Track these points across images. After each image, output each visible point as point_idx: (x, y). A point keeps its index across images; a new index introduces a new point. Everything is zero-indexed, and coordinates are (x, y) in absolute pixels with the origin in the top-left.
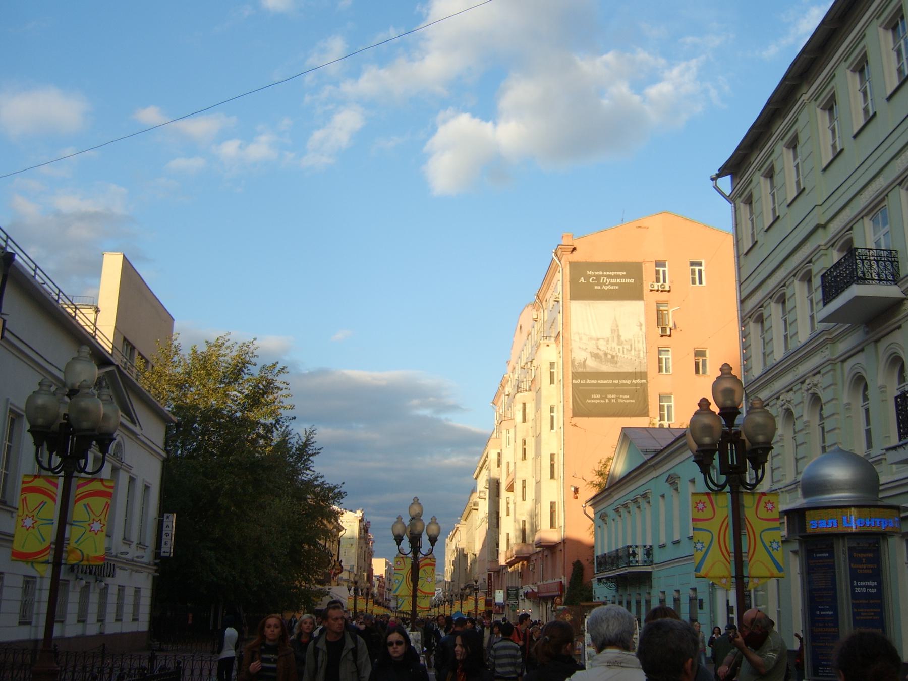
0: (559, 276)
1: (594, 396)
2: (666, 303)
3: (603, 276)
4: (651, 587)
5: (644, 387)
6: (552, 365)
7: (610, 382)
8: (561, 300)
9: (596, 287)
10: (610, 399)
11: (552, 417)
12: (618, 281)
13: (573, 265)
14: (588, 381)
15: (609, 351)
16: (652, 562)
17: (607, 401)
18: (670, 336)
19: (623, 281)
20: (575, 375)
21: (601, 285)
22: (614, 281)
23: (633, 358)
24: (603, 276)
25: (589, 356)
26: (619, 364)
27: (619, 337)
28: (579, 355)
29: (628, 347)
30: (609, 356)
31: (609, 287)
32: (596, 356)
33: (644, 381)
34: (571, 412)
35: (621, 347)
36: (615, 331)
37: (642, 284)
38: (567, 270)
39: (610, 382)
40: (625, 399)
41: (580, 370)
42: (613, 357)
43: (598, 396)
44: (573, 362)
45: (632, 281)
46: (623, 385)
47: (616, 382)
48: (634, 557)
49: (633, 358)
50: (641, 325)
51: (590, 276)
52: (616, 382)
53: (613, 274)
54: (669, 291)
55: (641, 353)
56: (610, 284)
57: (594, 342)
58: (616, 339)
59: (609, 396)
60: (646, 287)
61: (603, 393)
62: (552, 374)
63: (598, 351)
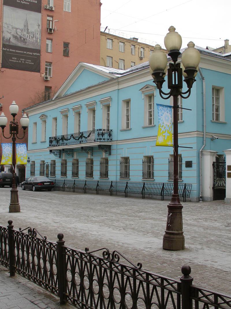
4: (110, 154)
5: (39, 57)
7: (22, 52)
10: (21, 61)
14: (11, 50)
15: (22, 36)
16: (111, 140)
20: (4, 46)
23: (34, 42)
25: (12, 37)
26: (27, 44)
27: (28, 30)
28: (7, 36)
29: (32, 36)
30: (22, 39)
32: (15, 37)
33: (39, 54)
36: (26, 26)
39: (22, 52)
40: (29, 62)
41: (7, 43)
42: (24, 39)
43: (16, 59)
44: (3, 38)
45: (36, 2)
47: (25, 52)
48: (103, 136)
49: (34, 42)
52: (25, 52)
55: (38, 40)
58: (26, 30)
59: (22, 60)
61: (19, 57)
63: (17, 35)
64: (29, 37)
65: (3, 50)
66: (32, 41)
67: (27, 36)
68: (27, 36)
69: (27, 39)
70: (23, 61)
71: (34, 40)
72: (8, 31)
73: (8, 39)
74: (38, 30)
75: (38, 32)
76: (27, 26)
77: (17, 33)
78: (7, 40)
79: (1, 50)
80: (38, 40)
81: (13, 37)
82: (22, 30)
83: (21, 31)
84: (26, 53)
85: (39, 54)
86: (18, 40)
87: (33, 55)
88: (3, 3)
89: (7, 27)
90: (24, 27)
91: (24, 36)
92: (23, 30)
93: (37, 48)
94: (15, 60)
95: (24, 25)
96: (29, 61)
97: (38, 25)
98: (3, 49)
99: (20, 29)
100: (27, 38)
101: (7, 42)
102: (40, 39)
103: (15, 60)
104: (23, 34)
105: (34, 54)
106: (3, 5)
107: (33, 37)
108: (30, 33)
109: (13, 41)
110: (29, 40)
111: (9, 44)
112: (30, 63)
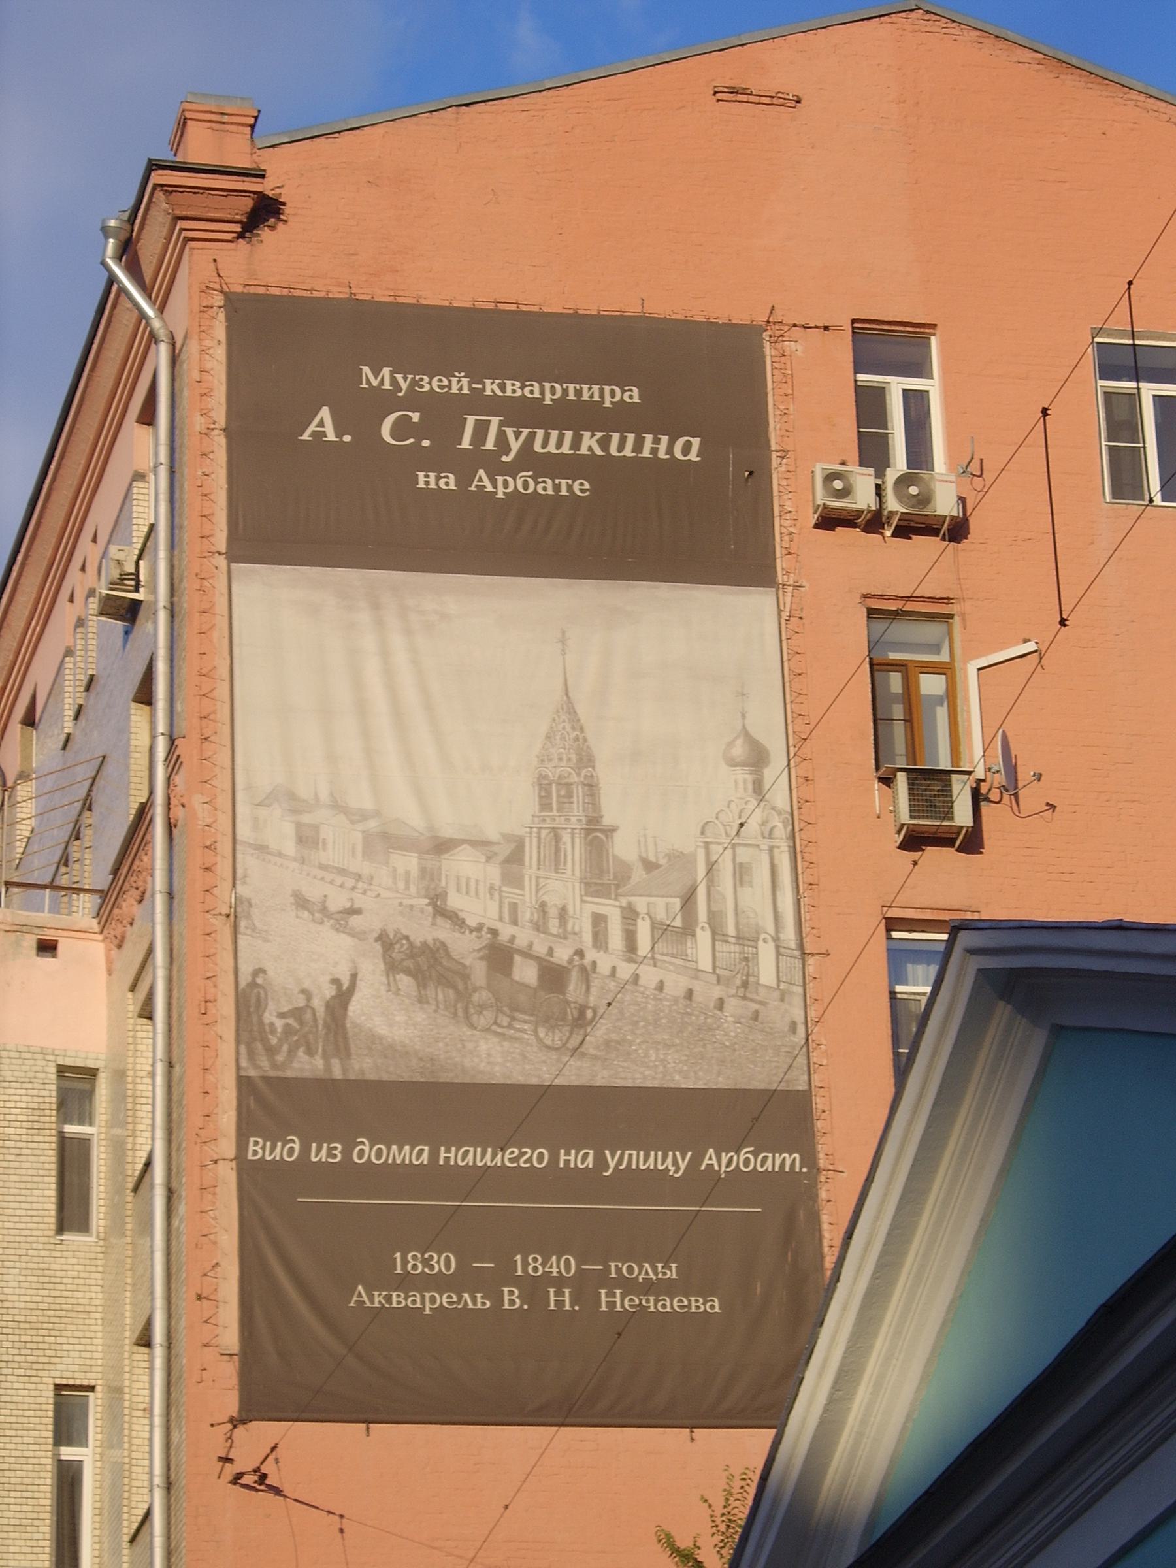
0: (143, 447)
1: (409, 1262)
2: (937, 612)
3: (478, 403)
6: (75, 1087)
7: (535, 1157)
8: (156, 593)
9: (425, 480)
10: (534, 1288)
11: (68, 1481)
12: (590, 443)
13: (263, 326)
14: (366, 1151)
15: (523, 936)
17: (512, 1298)
18: (972, 842)
19: (622, 446)
20: (266, 1103)
21: (466, 465)
22: (553, 443)
24: (478, 403)
25: (372, 971)
26: (600, 1032)
27: (597, 833)
28: (300, 958)
29: (666, 907)
30: (526, 973)
31: (521, 482)
32: (420, 966)
34: (229, 1372)
35: (612, 910)
37: (756, 475)
38: (212, 357)
39: (535, 1157)
40: (649, 1289)
41: (307, 1065)
42: (553, 977)
43: (442, 1263)
44: (248, 1003)
45: (689, 449)
46: (634, 1183)
47: (580, 1159)
50: (757, 758)
51: (386, 401)
52: (580, 1159)
53: (549, 393)
54: (957, 530)
55: (766, 954)
56: (528, 460)
57: (409, 863)
58: (574, 850)
59: (533, 1265)
60: (794, 498)
62: (72, 1161)
63: (443, 932)
64: (616, 940)
65: (248, 1171)
66: (676, 984)
67: (599, 920)
68: (599, 920)
69: (587, 973)
70: (559, 1282)
71: (705, 964)
72: (313, 892)
73: (318, 1004)
74: (753, 826)
75: (744, 855)
76: (579, 792)
77: (440, 910)
78: (297, 1013)
79: (228, 1175)
80: (766, 954)
81: (392, 967)
82: (515, 857)
83: (494, 873)
84: (601, 1162)
85: (790, 1160)
86: (464, 996)
87: (704, 1185)
88: (221, 541)
89: (290, 847)
90: (545, 805)
91: (540, 927)
92: (531, 853)
93: (760, 1076)
94: (439, 1283)
95: (543, 786)
96: (647, 1271)
97: (739, 750)
98: (257, 1149)
99: (479, 844)
100: (591, 955)
101: (310, 1052)
102: (789, 935)
103: (439, 1283)
104: (527, 898)
105: (715, 1160)
106: (222, 562)
107: (688, 930)
108: (639, 874)
109: (395, 1026)
110: (626, 971)
111: (337, 1074)
112: (671, 1304)
